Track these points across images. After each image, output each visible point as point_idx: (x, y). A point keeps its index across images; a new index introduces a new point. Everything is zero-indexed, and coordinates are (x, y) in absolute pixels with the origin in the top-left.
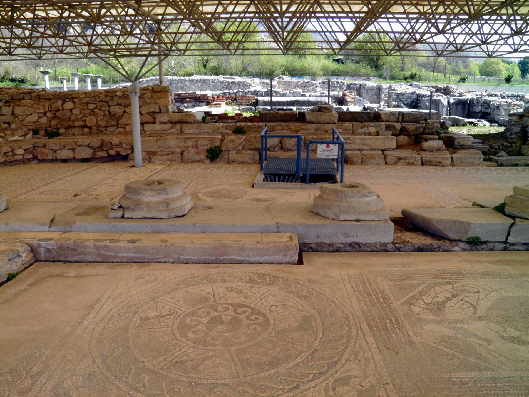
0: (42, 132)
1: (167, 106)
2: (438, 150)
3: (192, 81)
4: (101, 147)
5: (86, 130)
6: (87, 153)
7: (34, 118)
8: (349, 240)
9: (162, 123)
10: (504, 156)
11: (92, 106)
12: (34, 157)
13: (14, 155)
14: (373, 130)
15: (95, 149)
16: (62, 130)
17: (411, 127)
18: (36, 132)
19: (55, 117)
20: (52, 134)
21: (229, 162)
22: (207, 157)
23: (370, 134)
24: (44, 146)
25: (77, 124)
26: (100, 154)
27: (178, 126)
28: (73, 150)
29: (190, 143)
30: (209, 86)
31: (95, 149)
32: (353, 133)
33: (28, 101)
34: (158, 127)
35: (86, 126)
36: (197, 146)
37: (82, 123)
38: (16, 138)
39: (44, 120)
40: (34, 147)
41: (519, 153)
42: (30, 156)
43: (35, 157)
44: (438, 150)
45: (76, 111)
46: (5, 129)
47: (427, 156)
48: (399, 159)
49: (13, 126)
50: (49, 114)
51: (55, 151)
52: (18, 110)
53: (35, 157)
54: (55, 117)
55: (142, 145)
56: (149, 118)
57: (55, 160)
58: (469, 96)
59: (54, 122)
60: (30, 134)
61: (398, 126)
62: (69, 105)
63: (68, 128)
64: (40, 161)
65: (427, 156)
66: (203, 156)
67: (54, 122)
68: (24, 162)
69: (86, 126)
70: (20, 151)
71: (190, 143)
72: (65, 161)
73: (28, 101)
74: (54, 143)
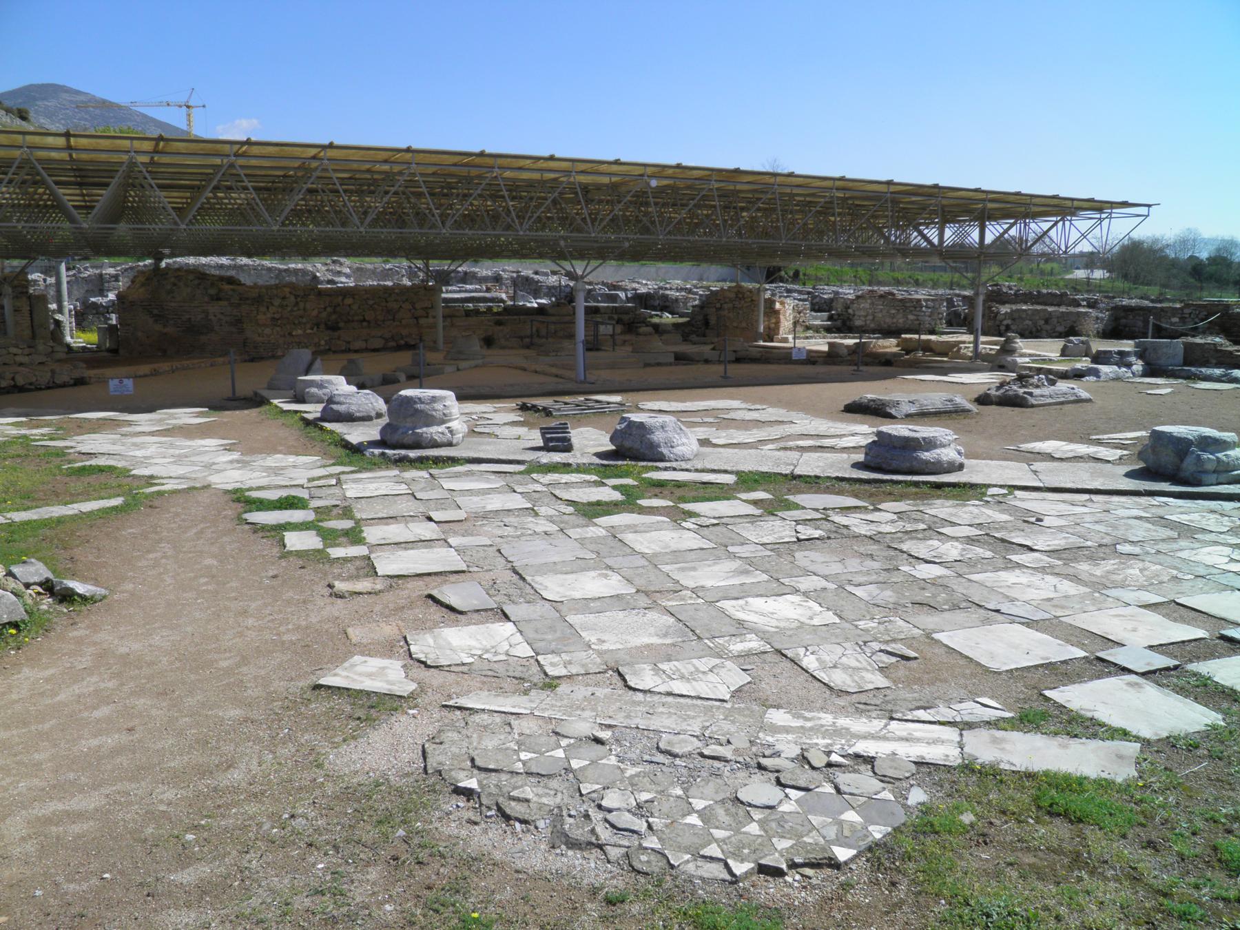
2: (650, 334)
4: (393, 338)
5: (365, 324)
6: (378, 343)
10: (694, 337)
11: (371, 302)
15: (387, 340)
16: (341, 325)
17: (626, 318)
19: (335, 312)
21: (503, 348)
28: (366, 341)
31: (387, 340)
35: (364, 320)
39: (324, 315)
41: (704, 336)
44: (650, 334)
45: (355, 307)
50: (329, 309)
51: (349, 342)
54: (335, 312)
58: (643, 290)
59: (334, 317)
61: (616, 317)
62: (348, 301)
64: (335, 352)
67: (334, 317)
69: (364, 320)
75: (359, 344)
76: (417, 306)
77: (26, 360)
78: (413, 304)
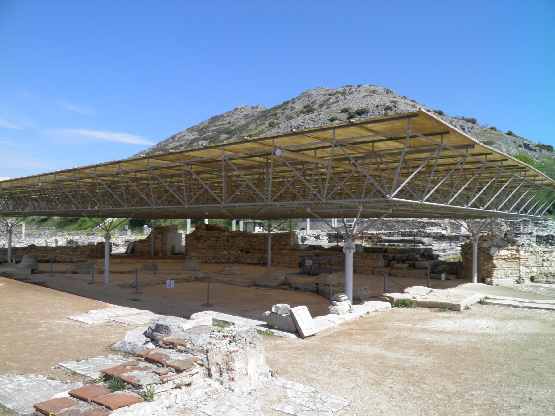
0: (244, 251)
1: (290, 241)
3: (398, 221)
4: (261, 259)
6: (256, 261)
7: (242, 244)
8: (266, 284)
9: (288, 250)
11: (263, 241)
12: (238, 261)
13: (230, 259)
14: (375, 257)
16: (251, 251)
18: (242, 251)
19: (250, 245)
20: (248, 252)
22: (298, 266)
23: (373, 259)
24: (242, 257)
25: (257, 248)
26: (261, 262)
27: (293, 252)
28: (252, 259)
29: (293, 259)
30: (410, 225)
31: (259, 260)
32: (366, 258)
33: (241, 237)
34: (286, 251)
35: (260, 249)
36: (295, 261)
37: (258, 248)
38: (233, 253)
39: (246, 246)
40: (239, 257)
42: (236, 261)
43: (238, 261)
45: (257, 243)
46: (230, 249)
47: (393, 271)
48: (379, 272)
49: (233, 248)
50: (248, 243)
52: (236, 241)
53: (238, 261)
54: (250, 245)
55: (354, 266)
56: (283, 247)
57: (245, 263)
60: (239, 252)
62: (255, 240)
63: (254, 249)
64: (240, 263)
65: (393, 271)
66: (296, 266)
67: (249, 247)
68: (233, 263)
69: (260, 249)
70: (232, 258)
71: (293, 259)
72: (249, 264)
73: (241, 237)
74: (245, 256)
75: (249, 261)
76: (282, 243)
77: (71, 253)
78: (279, 242)
